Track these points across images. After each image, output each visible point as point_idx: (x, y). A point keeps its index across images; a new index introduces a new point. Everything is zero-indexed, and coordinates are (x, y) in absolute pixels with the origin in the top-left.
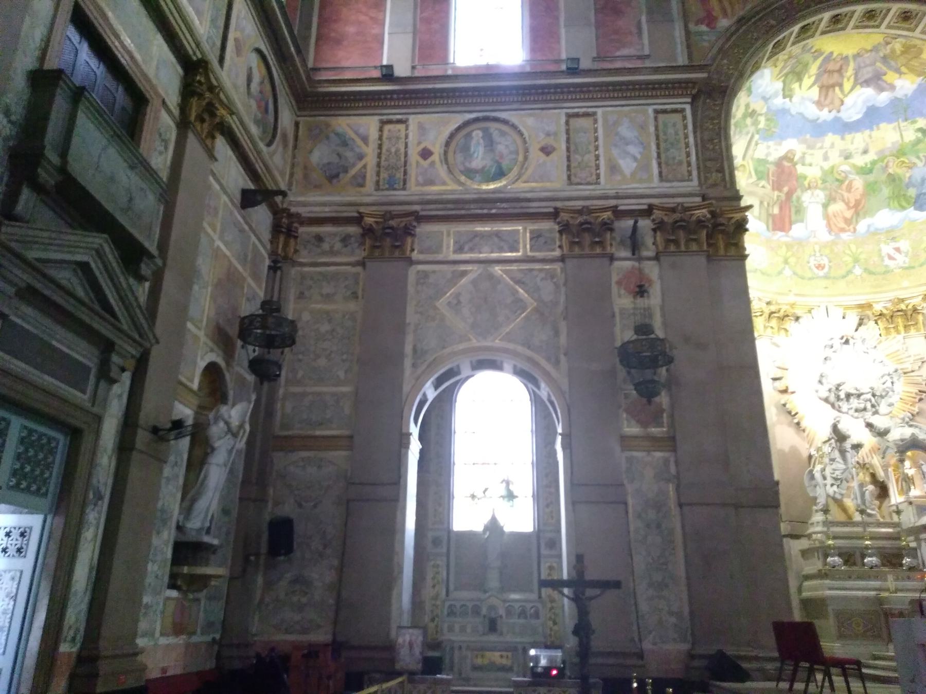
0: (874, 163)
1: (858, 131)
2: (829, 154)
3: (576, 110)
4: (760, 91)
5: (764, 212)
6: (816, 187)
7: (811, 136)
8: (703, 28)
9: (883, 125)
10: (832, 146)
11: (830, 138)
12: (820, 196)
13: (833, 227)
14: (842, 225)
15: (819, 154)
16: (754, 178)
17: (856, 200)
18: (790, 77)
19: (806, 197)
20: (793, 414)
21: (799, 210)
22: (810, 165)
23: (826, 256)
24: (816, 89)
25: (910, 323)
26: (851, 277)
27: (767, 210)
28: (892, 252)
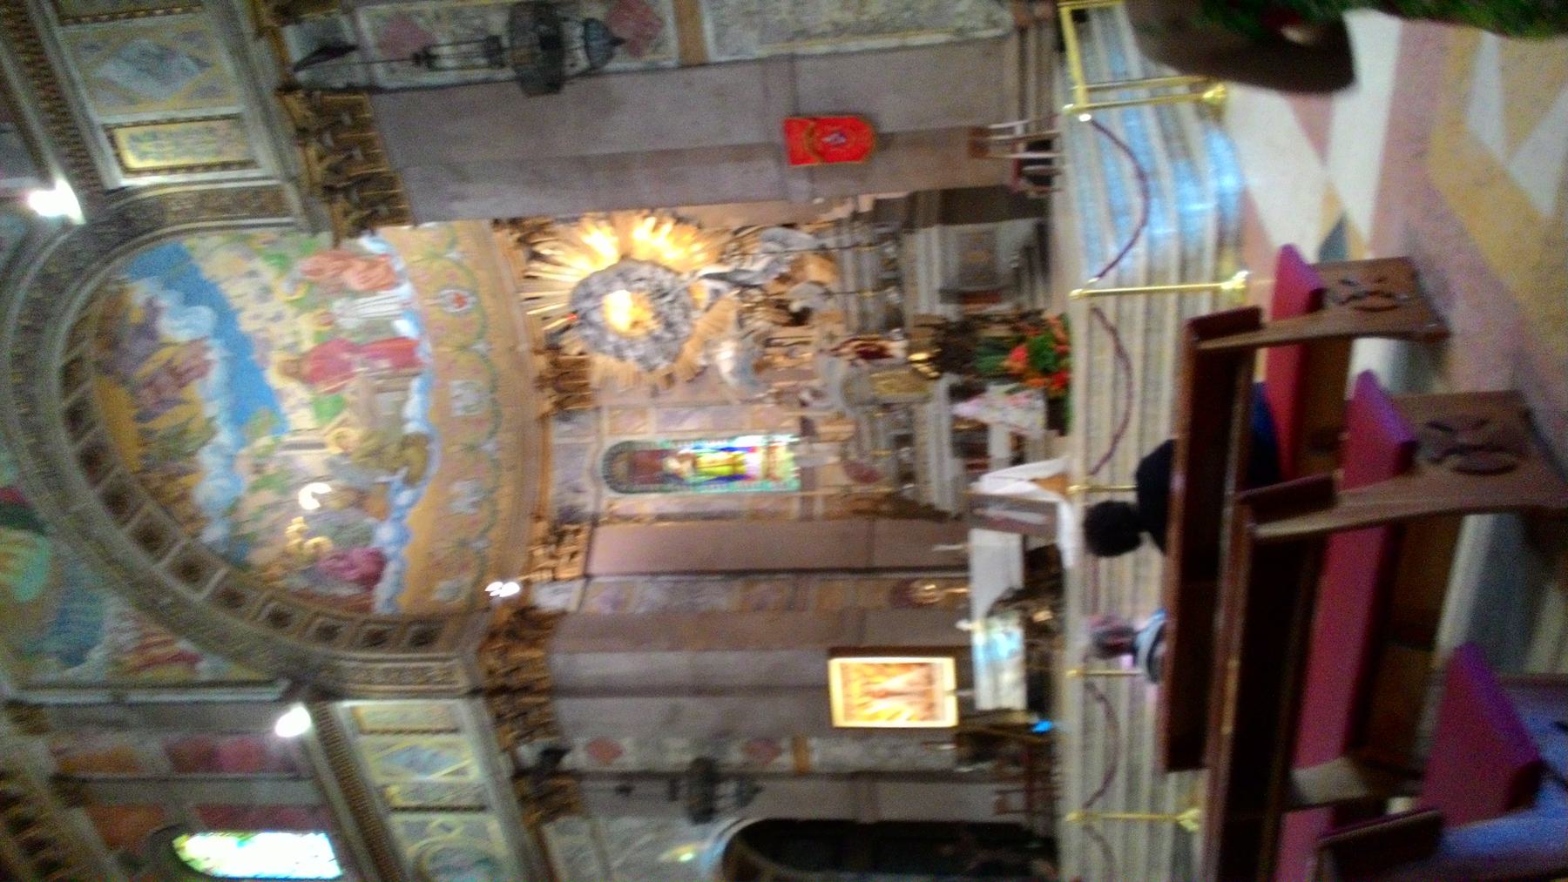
0: (268, 257)
5: (394, 384)
10: (256, 317)
11: (247, 324)
12: (338, 305)
14: (380, 271)
16: (346, 414)
18: (189, 448)
19: (349, 322)
21: (374, 326)
24: (186, 393)
26: (466, 262)
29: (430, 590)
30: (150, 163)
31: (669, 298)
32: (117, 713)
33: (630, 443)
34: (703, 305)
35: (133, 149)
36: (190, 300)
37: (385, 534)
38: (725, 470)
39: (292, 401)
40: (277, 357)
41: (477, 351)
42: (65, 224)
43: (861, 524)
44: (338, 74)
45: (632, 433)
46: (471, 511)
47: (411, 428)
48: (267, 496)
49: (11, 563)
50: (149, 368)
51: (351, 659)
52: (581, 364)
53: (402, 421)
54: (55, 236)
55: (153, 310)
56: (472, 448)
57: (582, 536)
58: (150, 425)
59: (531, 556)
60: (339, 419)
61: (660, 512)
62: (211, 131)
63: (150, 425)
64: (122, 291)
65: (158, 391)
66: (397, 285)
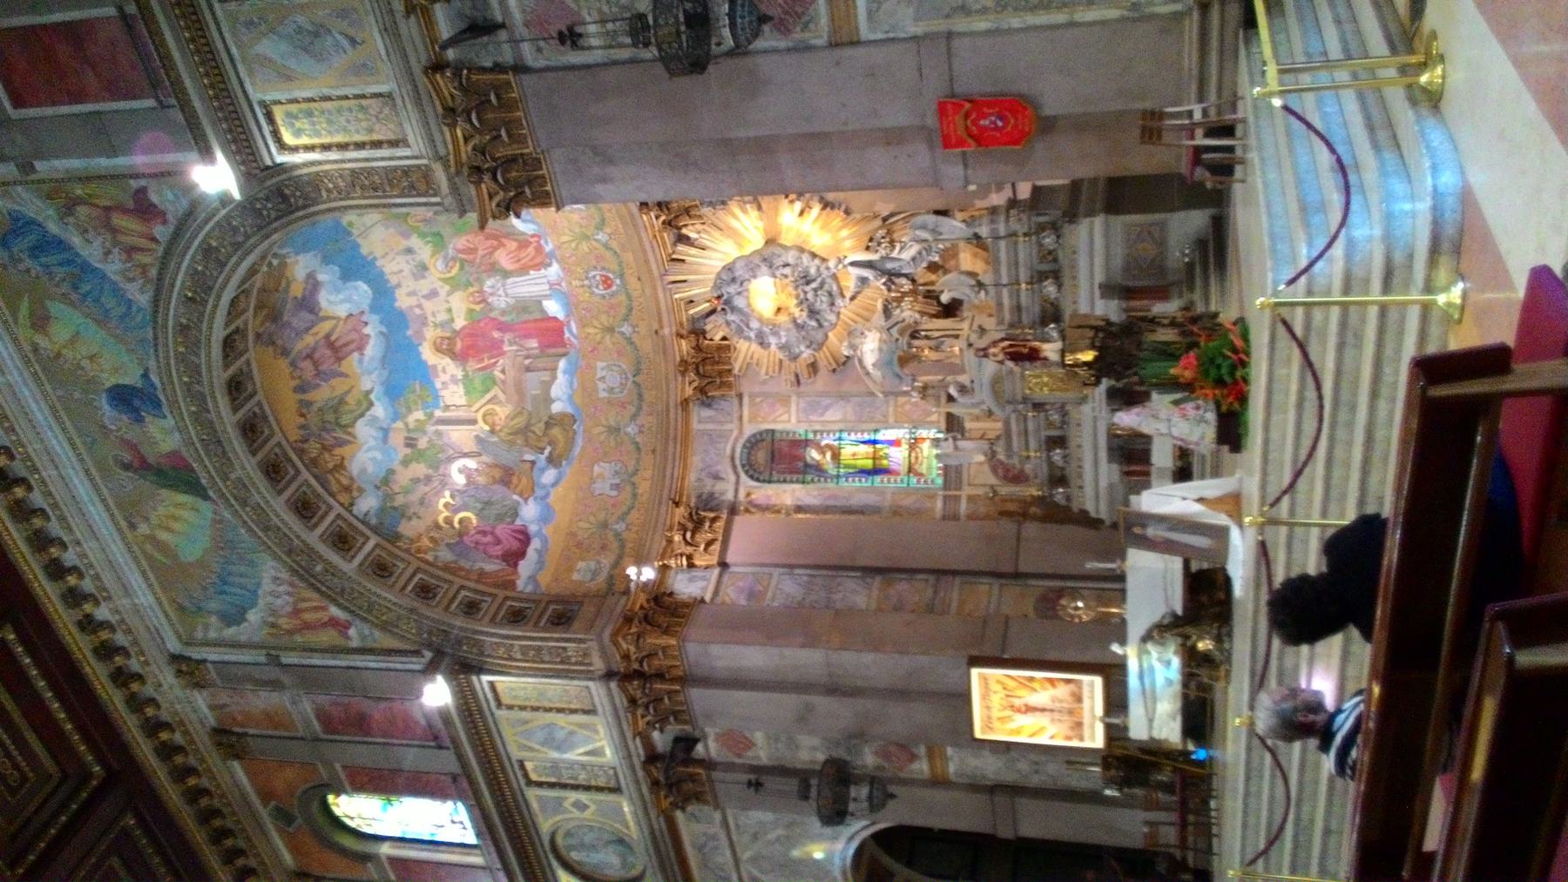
0: (422, 235)
1: (382, 274)
2: (425, 292)
3: (520, 778)
4: (378, 455)
5: (540, 363)
6: (481, 292)
7: (407, 328)
8: (352, 632)
9: (364, 251)
10: (411, 294)
11: (403, 301)
13: (538, 260)
14: (531, 250)
15: (429, 306)
16: (495, 391)
17: (487, 239)
18: (345, 420)
19: (500, 302)
22: (450, 310)
23: (587, 272)
26: (614, 245)
27: (537, 357)
29: (570, 570)
30: (305, 140)
31: (814, 285)
32: (273, 673)
33: (773, 431)
34: (848, 295)
35: (292, 125)
36: (347, 275)
37: (529, 512)
38: (869, 464)
39: (444, 377)
40: (430, 333)
41: (622, 334)
42: (225, 199)
43: (1008, 526)
44: (486, 53)
45: (774, 421)
46: (614, 493)
47: (557, 408)
48: (419, 469)
49: (177, 526)
50: (309, 340)
51: (492, 635)
52: (725, 348)
53: (549, 401)
54: (218, 210)
55: (313, 285)
56: (614, 430)
57: (720, 525)
58: (308, 397)
59: (670, 541)
60: (488, 396)
61: (799, 503)
62: (362, 108)
63: (308, 397)
64: (283, 265)
65: (316, 364)
66: (550, 265)
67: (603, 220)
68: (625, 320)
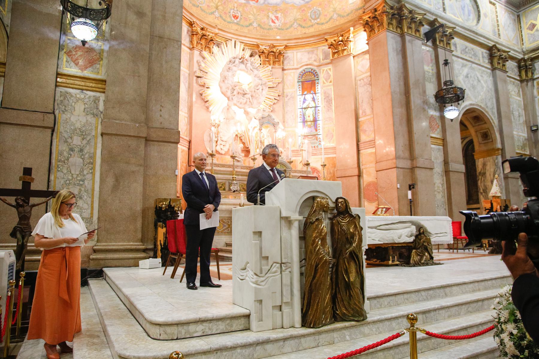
20: (206, 100)
23: (240, 12)
25: (276, 60)
26: (251, 27)
28: (274, 18)
67: (263, 29)
68: (220, 15)
